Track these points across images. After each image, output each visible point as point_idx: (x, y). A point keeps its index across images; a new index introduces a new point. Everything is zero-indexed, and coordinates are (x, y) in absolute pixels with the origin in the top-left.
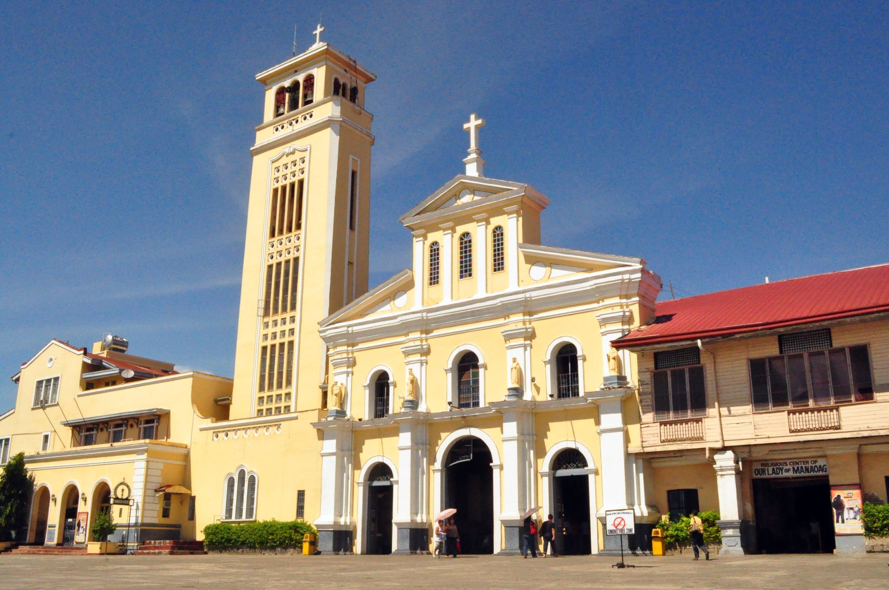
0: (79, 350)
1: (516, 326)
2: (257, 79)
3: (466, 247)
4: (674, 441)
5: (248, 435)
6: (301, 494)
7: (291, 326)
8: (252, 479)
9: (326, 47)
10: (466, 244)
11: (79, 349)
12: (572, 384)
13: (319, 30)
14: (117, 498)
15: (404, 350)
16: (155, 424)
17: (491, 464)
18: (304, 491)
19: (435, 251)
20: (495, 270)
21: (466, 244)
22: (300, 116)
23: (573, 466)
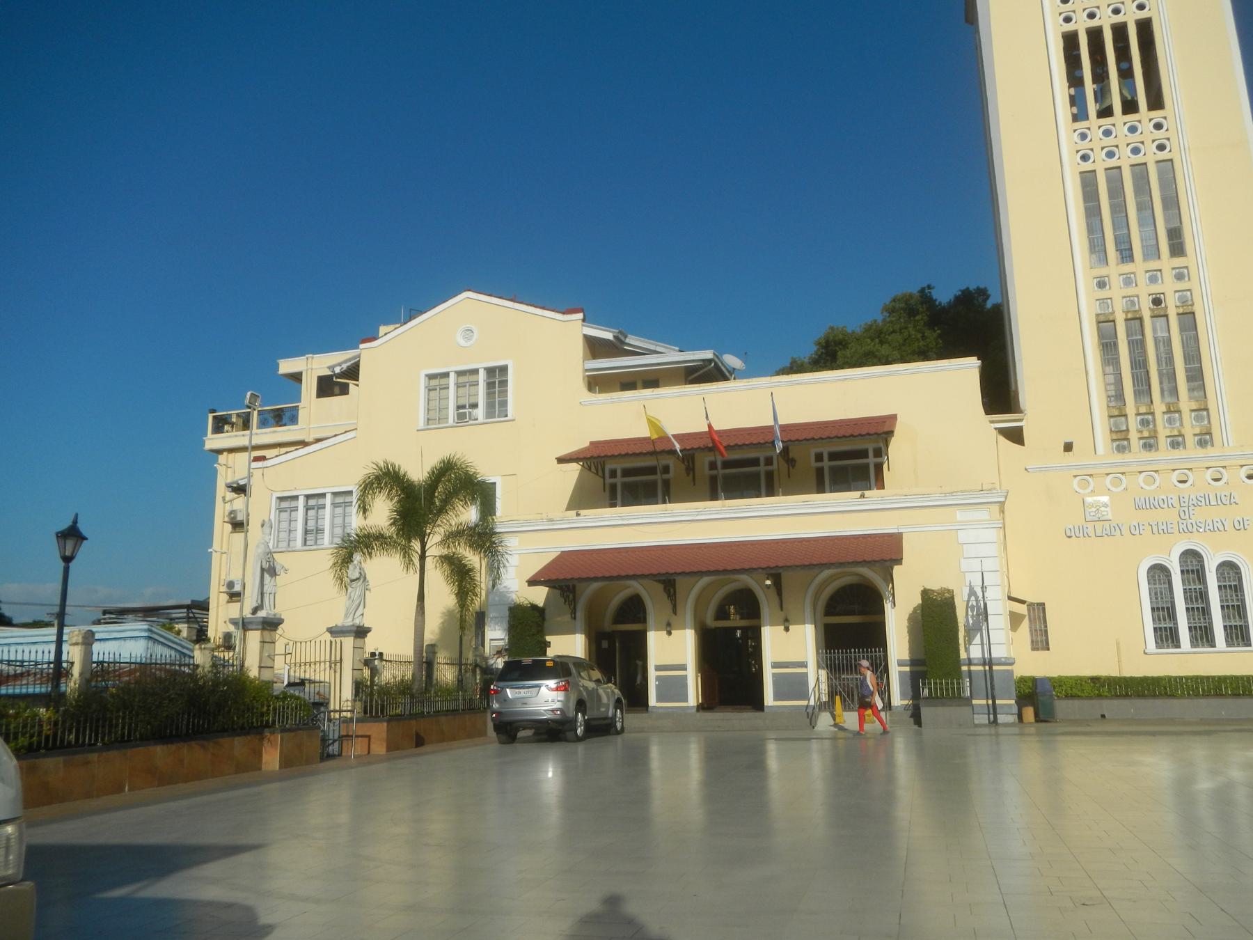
0: (564, 313)
11: (563, 311)
16: (871, 460)
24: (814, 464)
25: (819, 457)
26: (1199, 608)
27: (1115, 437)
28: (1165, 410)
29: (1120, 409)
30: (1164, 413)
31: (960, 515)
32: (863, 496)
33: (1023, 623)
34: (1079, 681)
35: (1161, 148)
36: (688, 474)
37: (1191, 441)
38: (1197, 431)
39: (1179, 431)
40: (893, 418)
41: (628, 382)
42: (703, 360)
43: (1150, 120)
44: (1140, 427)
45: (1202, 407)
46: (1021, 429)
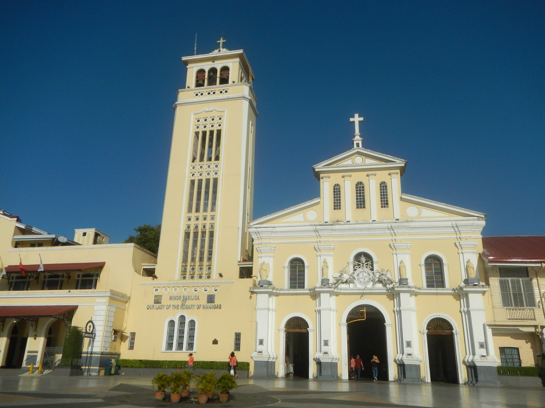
1: (401, 241)
2: (182, 59)
3: (360, 190)
4: (516, 319)
5: (167, 292)
6: (238, 337)
7: (212, 222)
8: (192, 323)
9: (242, 52)
10: (360, 188)
12: (435, 279)
13: (221, 41)
14: (86, 333)
15: (317, 247)
16: (94, 278)
17: (385, 324)
18: (240, 333)
19: (337, 191)
20: (382, 207)
21: (360, 188)
22: (217, 89)
23: (440, 328)
24: (76, 278)
25: (79, 276)
26: (181, 337)
27: (182, 274)
28: (199, 265)
29: (186, 264)
30: (199, 266)
31: (98, 300)
32: (69, 292)
33: (127, 340)
34: (135, 361)
35: (216, 173)
36: (36, 280)
37: (204, 276)
38: (207, 273)
39: (202, 273)
40: (105, 262)
41: (33, 244)
42: (53, 238)
43: (214, 164)
44: (191, 270)
45: (210, 264)
46: (155, 268)
